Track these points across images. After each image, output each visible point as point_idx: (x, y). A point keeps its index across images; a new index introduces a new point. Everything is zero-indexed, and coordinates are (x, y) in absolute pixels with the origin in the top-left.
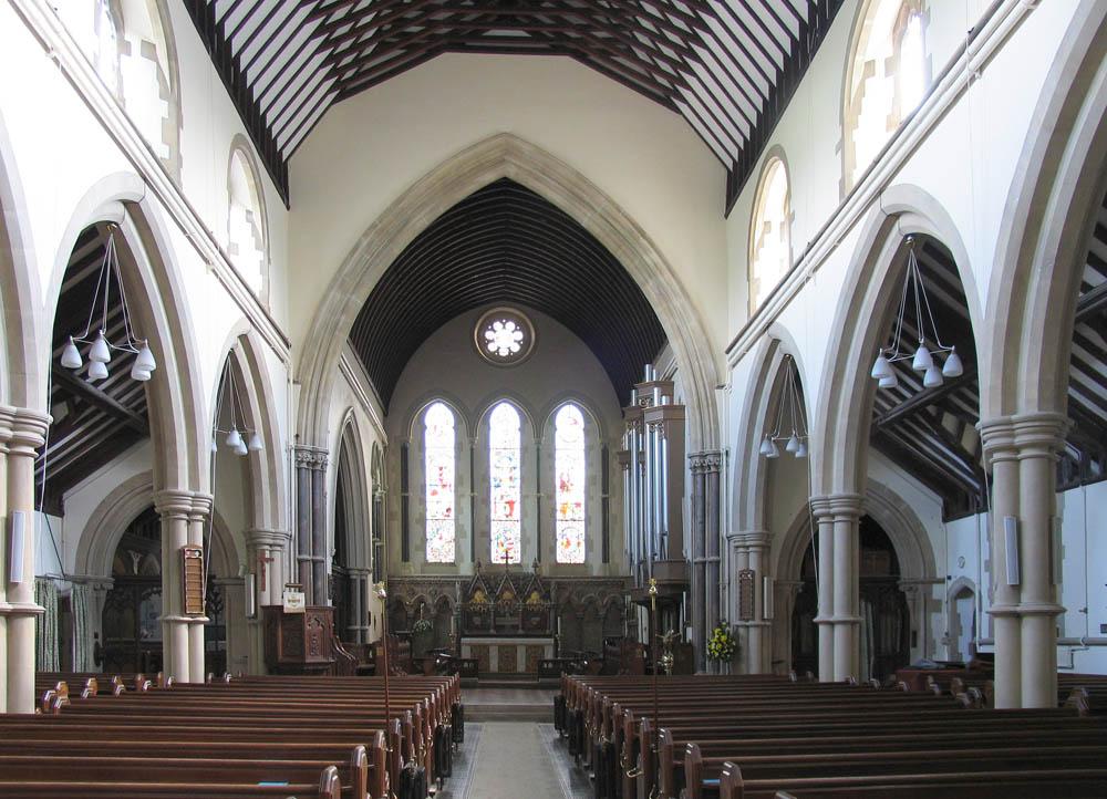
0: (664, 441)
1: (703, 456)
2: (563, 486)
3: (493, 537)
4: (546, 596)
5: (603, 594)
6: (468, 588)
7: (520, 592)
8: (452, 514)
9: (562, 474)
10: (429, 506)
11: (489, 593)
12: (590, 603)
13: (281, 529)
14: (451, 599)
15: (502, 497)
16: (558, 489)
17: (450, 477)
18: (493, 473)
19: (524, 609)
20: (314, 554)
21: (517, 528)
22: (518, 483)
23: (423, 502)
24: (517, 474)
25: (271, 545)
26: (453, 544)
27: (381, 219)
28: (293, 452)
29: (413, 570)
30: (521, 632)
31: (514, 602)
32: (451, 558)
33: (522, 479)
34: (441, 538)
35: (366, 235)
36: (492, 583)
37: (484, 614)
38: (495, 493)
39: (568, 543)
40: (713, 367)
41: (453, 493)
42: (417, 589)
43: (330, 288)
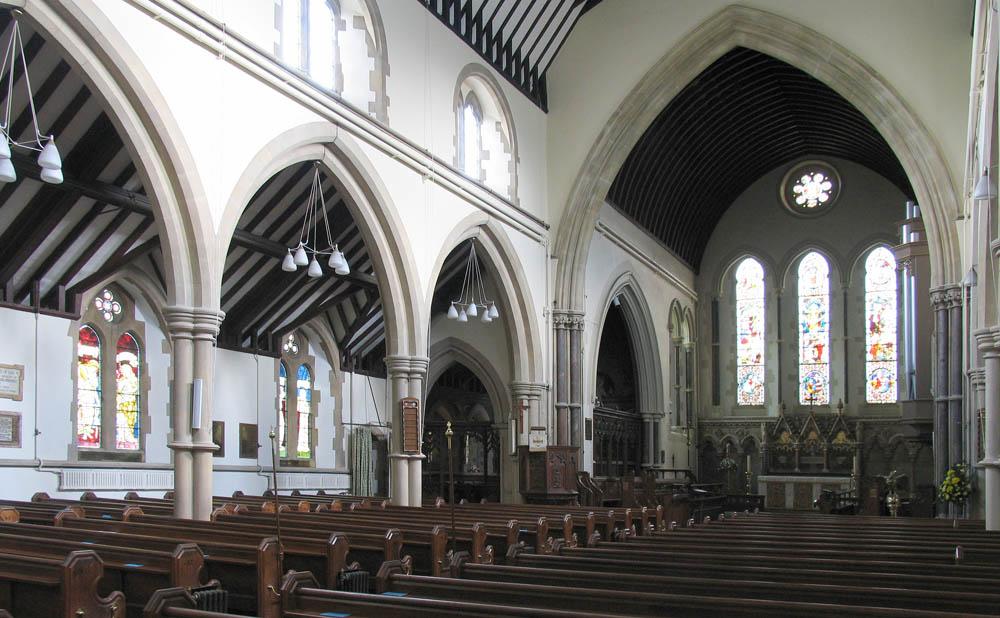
0: (913, 278)
1: (943, 291)
2: (874, 327)
3: (801, 380)
4: (852, 436)
6: (774, 430)
7: (824, 432)
8: (762, 360)
9: (872, 316)
10: (739, 353)
13: (537, 381)
15: (811, 342)
16: (868, 331)
17: (760, 326)
18: (802, 319)
20: (572, 402)
21: (826, 371)
22: (827, 327)
23: (734, 349)
24: (826, 318)
25: (528, 395)
26: (762, 388)
27: (621, 107)
28: (550, 316)
29: (716, 414)
32: (761, 400)
33: (831, 323)
34: (751, 383)
35: (609, 123)
37: (790, 454)
38: (803, 339)
39: (879, 384)
40: (953, 199)
41: (763, 341)
42: (724, 430)
43: (580, 175)
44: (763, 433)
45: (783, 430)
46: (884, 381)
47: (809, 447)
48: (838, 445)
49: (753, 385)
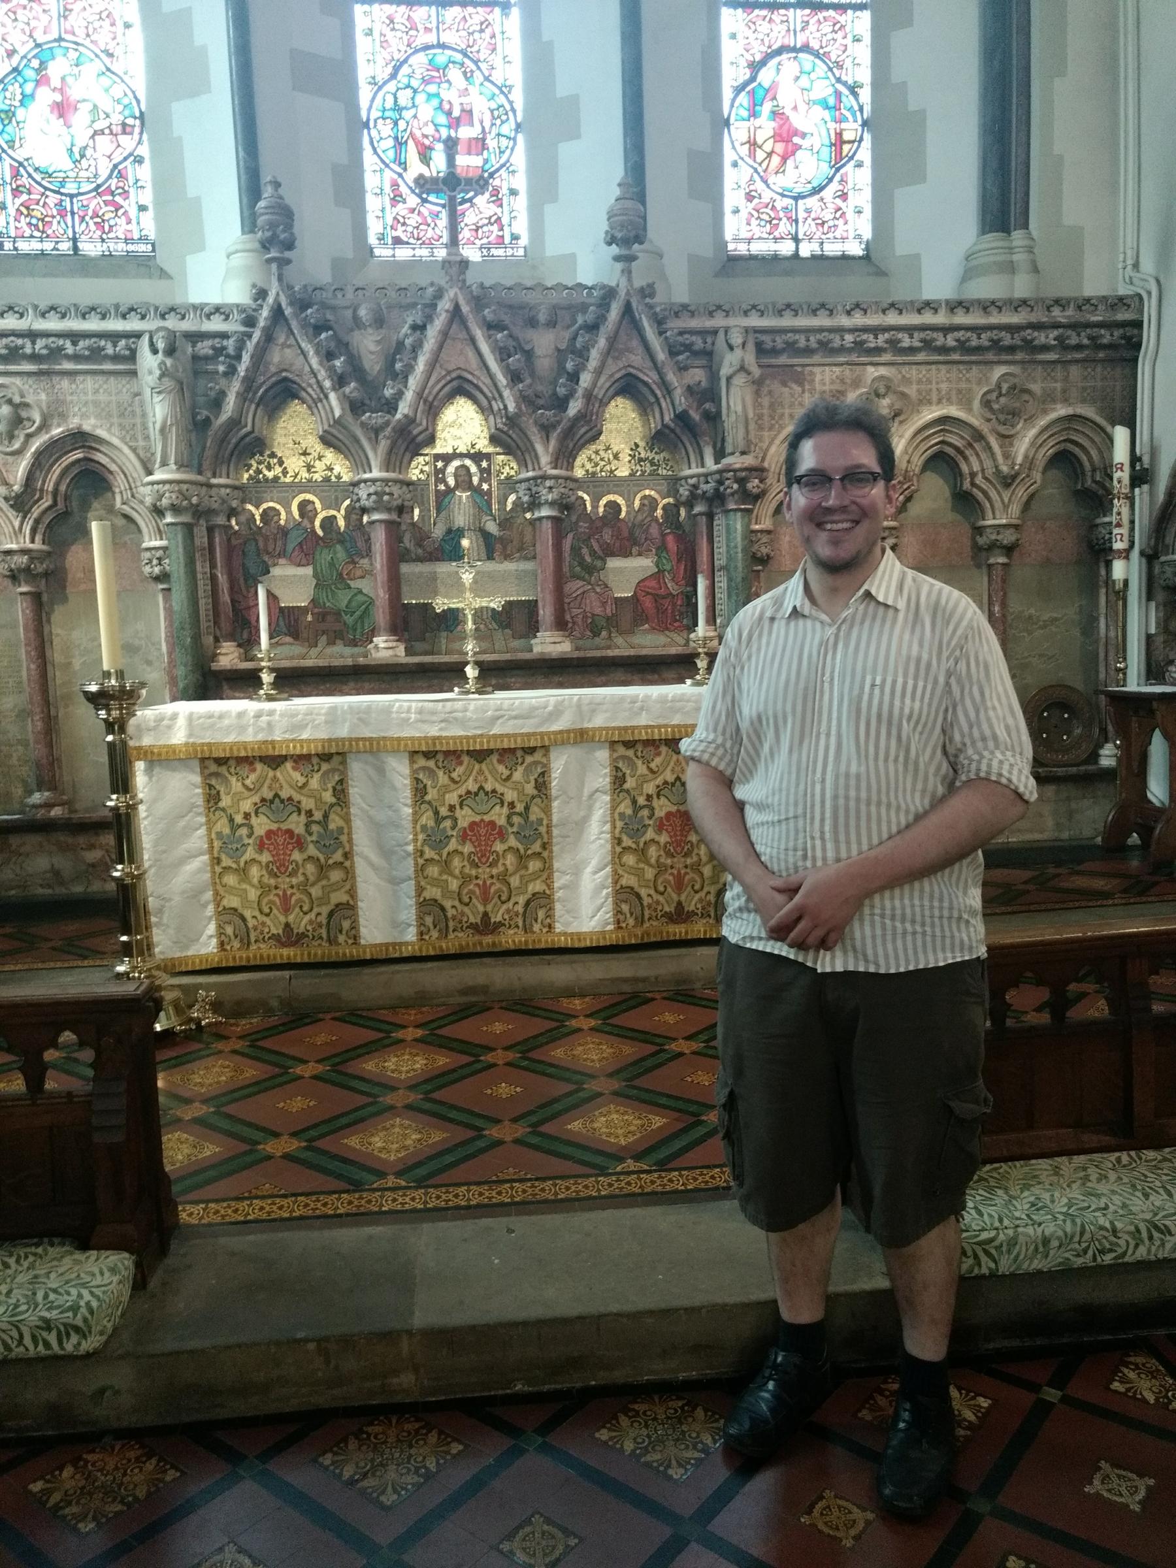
5: (1008, 409)
6: (227, 396)
11: (356, 407)
12: (942, 461)
14: (120, 457)
19: (565, 506)
30: (549, 643)
31: (506, 466)
36: (368, 345)
44: (159, 410)
45: (283, 392)
46: (814, 125)
47: (444, 497)
48: (612, 483)
49: (81, 119)
